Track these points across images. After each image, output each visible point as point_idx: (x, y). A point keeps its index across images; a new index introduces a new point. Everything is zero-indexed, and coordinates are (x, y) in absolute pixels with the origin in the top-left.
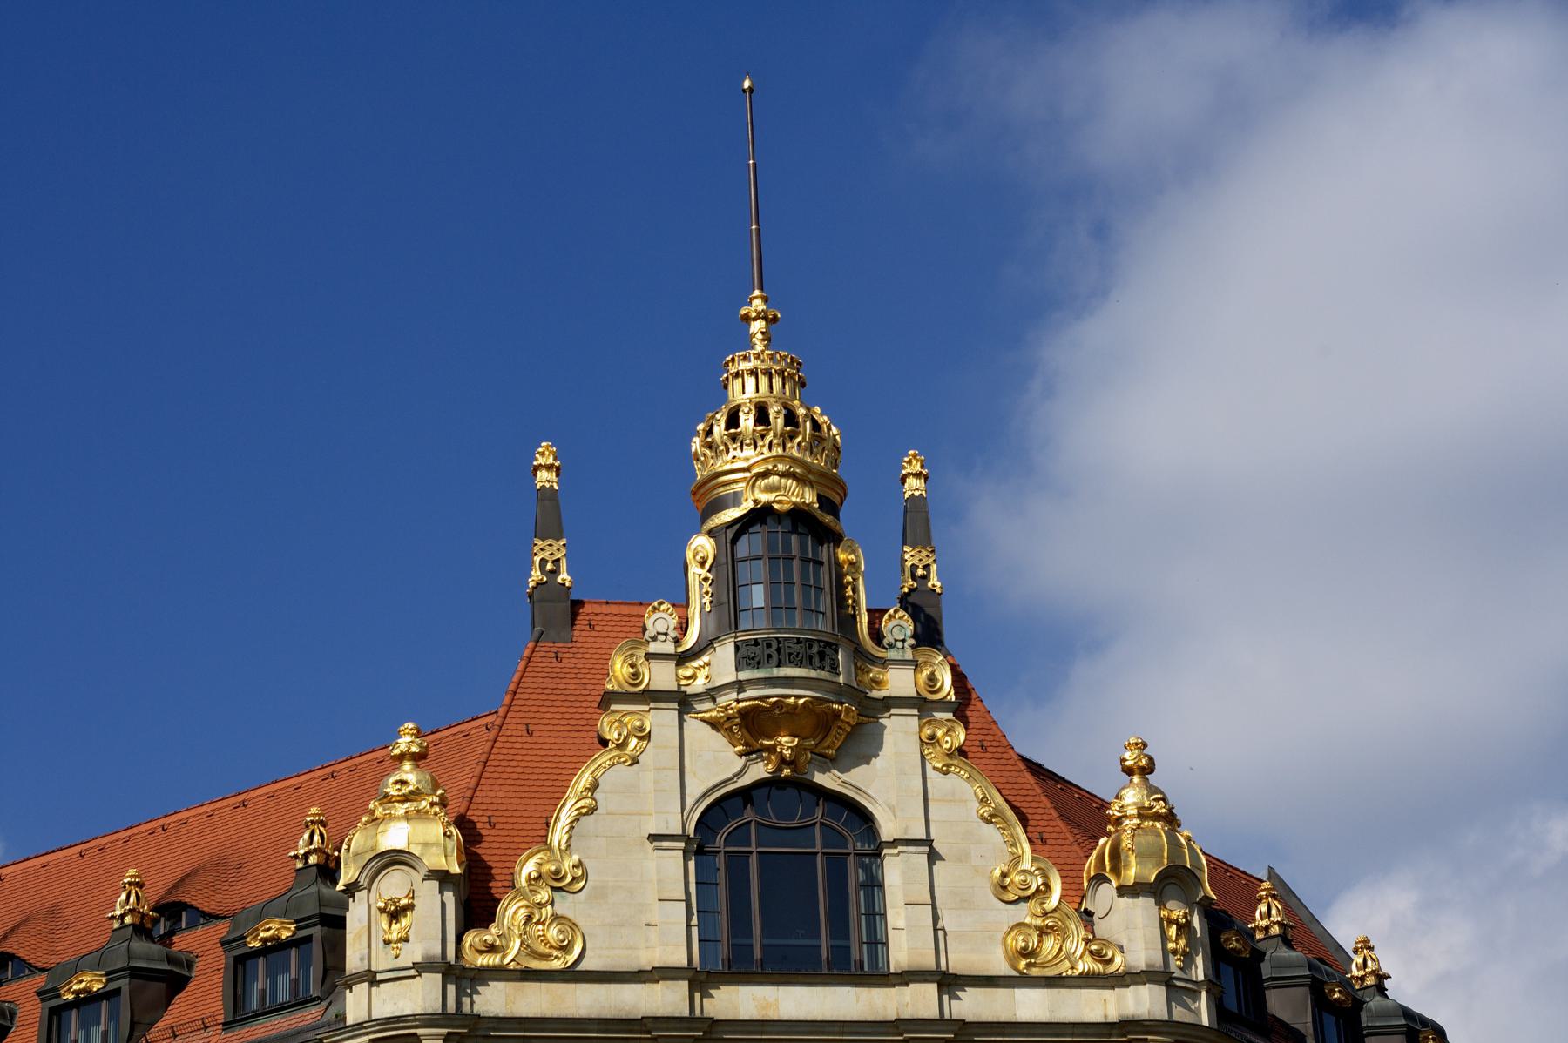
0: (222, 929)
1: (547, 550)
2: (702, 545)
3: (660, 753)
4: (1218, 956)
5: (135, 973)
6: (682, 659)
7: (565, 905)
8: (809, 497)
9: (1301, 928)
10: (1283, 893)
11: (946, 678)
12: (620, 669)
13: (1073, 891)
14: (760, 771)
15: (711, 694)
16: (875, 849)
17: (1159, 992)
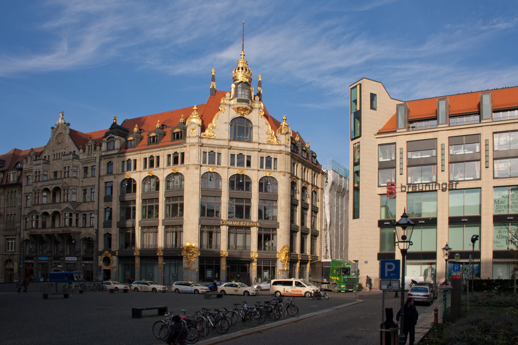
0: (171, 129)
1: (213, 83)
2: (233, 86)
3: (226, 112)
4: (292, 143)
5: (160, 134)
6: (230, 100)
7: (214, 130)
8: (248, 80)
9: (301, 140)
10: (299, 136)
11: (262, 105)
12: (222, 101)
13: (275, 135)
14: (239, 115)
15: (233, 105)
16: (251, 128)
17: (284, 147)
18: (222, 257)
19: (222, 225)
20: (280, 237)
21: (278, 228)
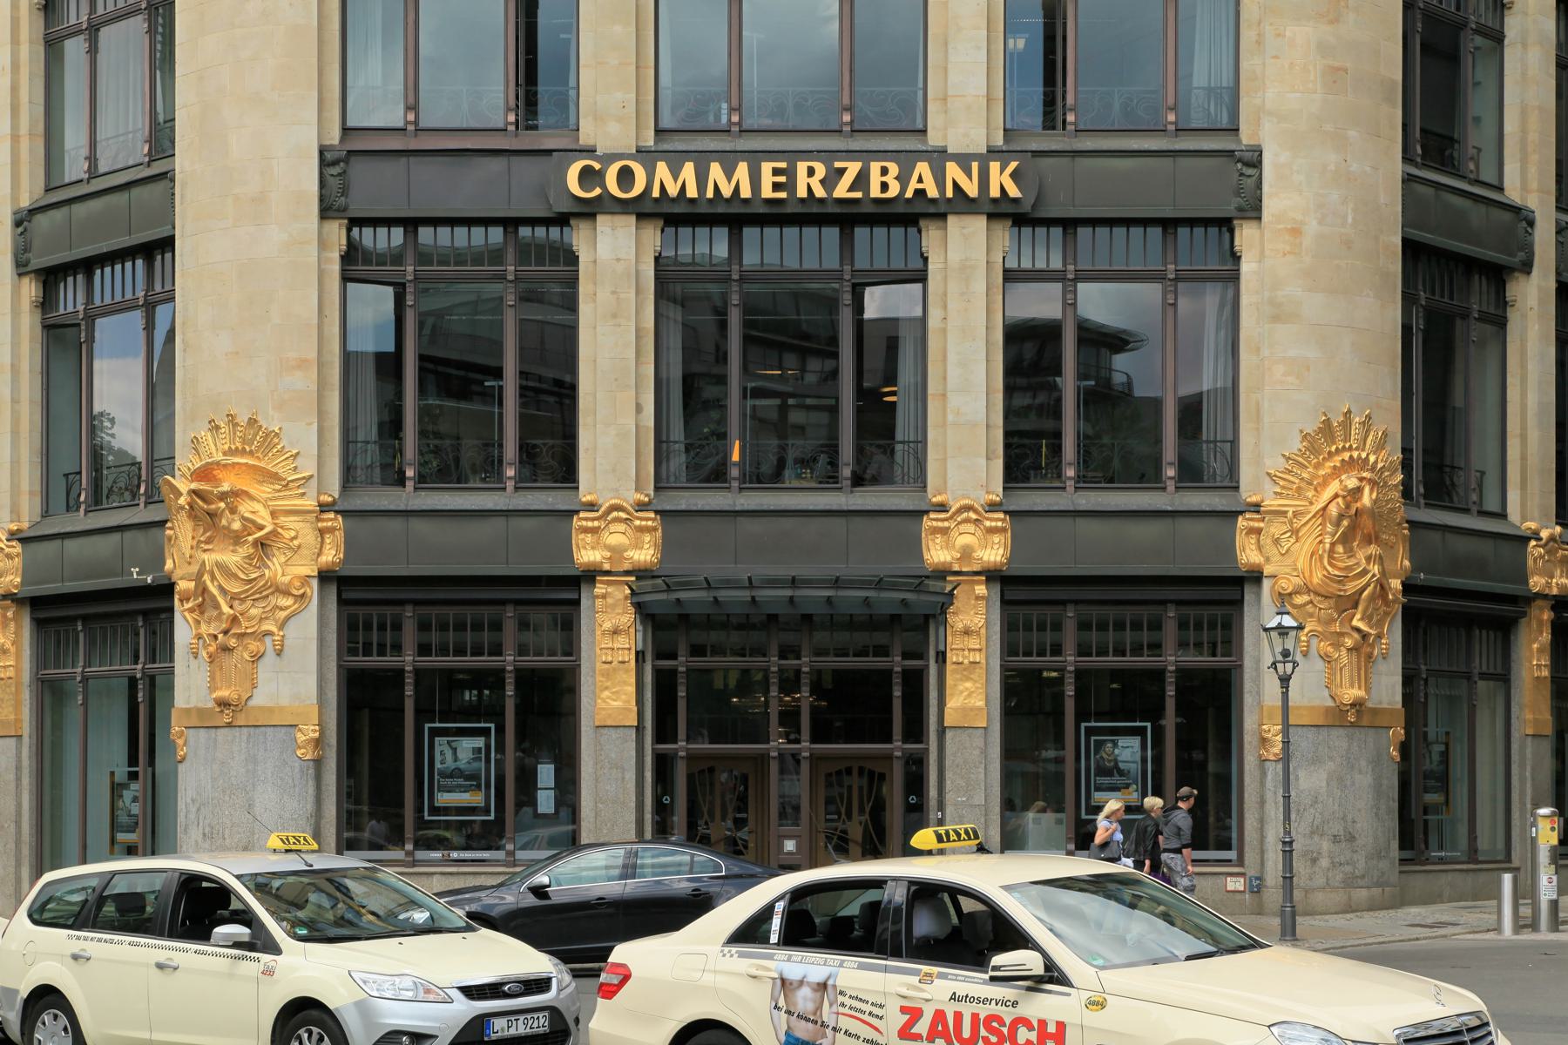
18: (590, 575)
19: (588, 211)
20: (1278, 314)
21: (1253, 210)
